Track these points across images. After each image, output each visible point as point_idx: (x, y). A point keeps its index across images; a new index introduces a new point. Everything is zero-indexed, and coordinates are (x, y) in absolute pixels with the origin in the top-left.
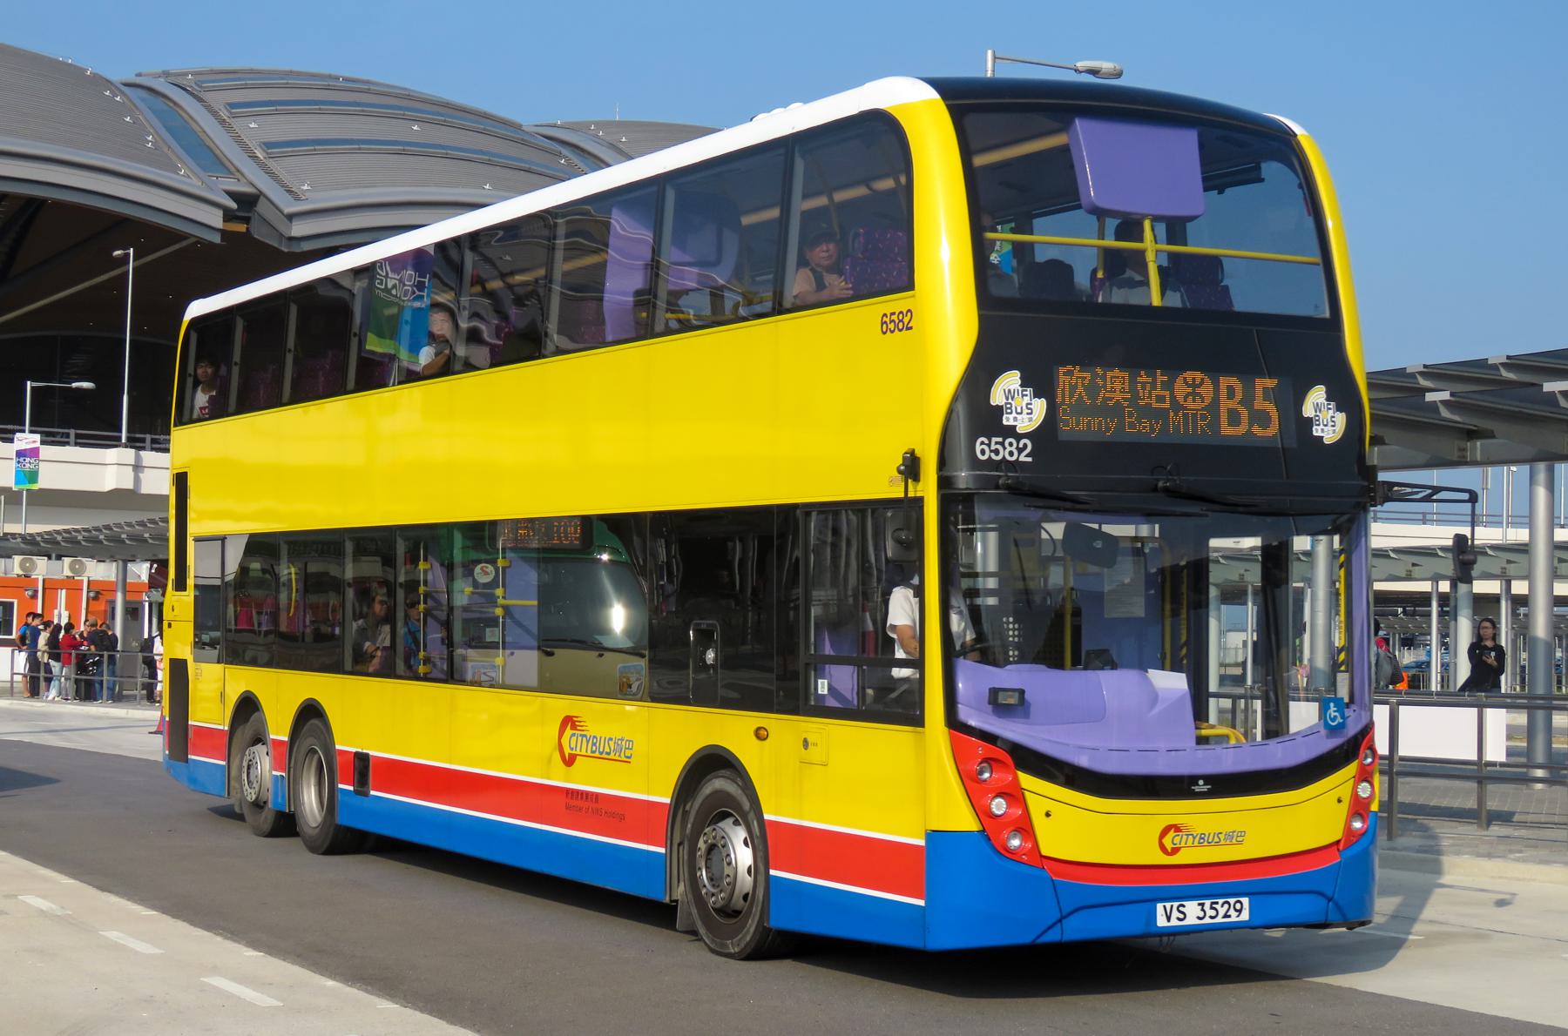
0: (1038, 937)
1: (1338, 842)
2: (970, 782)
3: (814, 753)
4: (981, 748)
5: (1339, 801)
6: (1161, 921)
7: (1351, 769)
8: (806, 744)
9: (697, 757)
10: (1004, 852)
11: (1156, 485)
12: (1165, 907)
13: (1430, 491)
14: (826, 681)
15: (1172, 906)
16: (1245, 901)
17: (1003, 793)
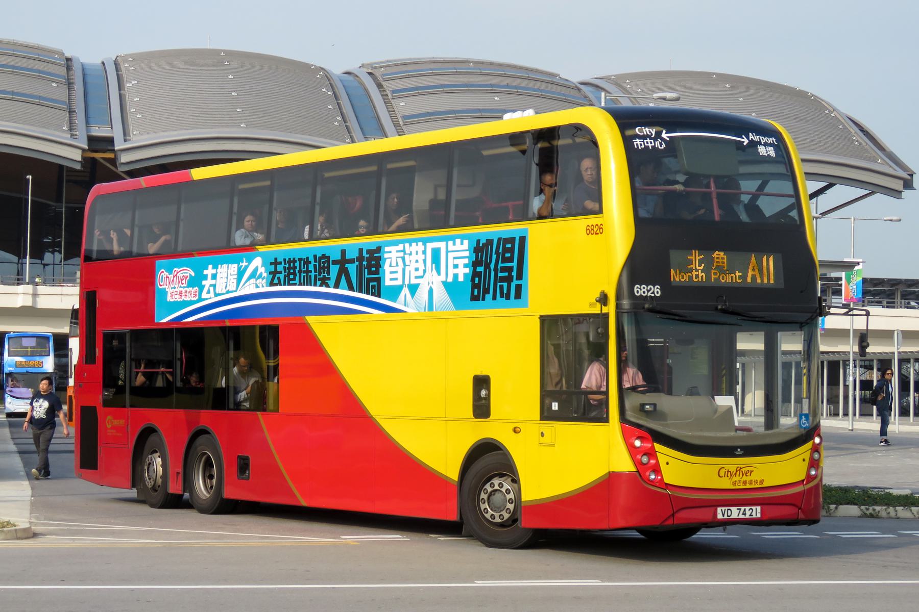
0: (664, 521)
1: (803, 481)
2: (631, 449)
3: (546, 439)
5: (804, 460)
6: (720, 516)
7: (809, 445)
8: (542, 435)
9: (480, 443)
10: (647, 481)
11: (716, 309)
12: (722, 510)
13: (848, 310)
14: (557, 404)
15: (725, 510)
16: (759, 508)
17: (648, 453)
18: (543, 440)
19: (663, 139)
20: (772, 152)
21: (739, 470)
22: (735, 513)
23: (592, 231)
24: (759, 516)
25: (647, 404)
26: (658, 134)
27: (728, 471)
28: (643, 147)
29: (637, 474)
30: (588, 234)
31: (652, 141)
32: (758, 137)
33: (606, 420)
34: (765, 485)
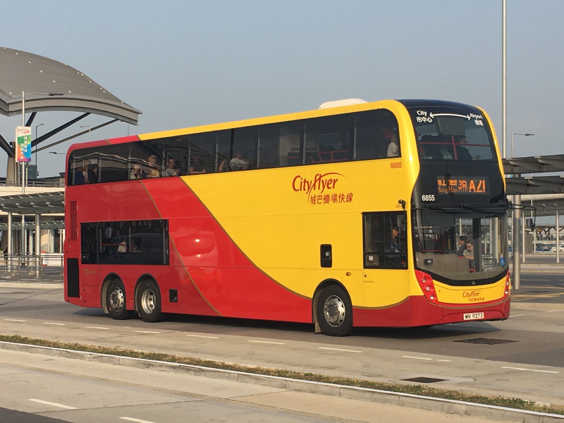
1: (503, 298)
2: (420, 282)
4: (424, 274)
6: (465, 319)
7: (505, 278)
8: (365, 276)
16: (483, 313)
18: (366, 279)
19: (431, 117)
20: (482, 124)
21: (473, 293)
22: (472, 316)
23: (395, 167)
24: (483, 317)
25: (429, 259)
26: (428, 115)
27: (468, 294)
28: (421, 121)
29: (424, 296)
30: (392, 168)
31: (426, 118)
32: (474, 115)
33: (406, 268)
34: (485, 301)
